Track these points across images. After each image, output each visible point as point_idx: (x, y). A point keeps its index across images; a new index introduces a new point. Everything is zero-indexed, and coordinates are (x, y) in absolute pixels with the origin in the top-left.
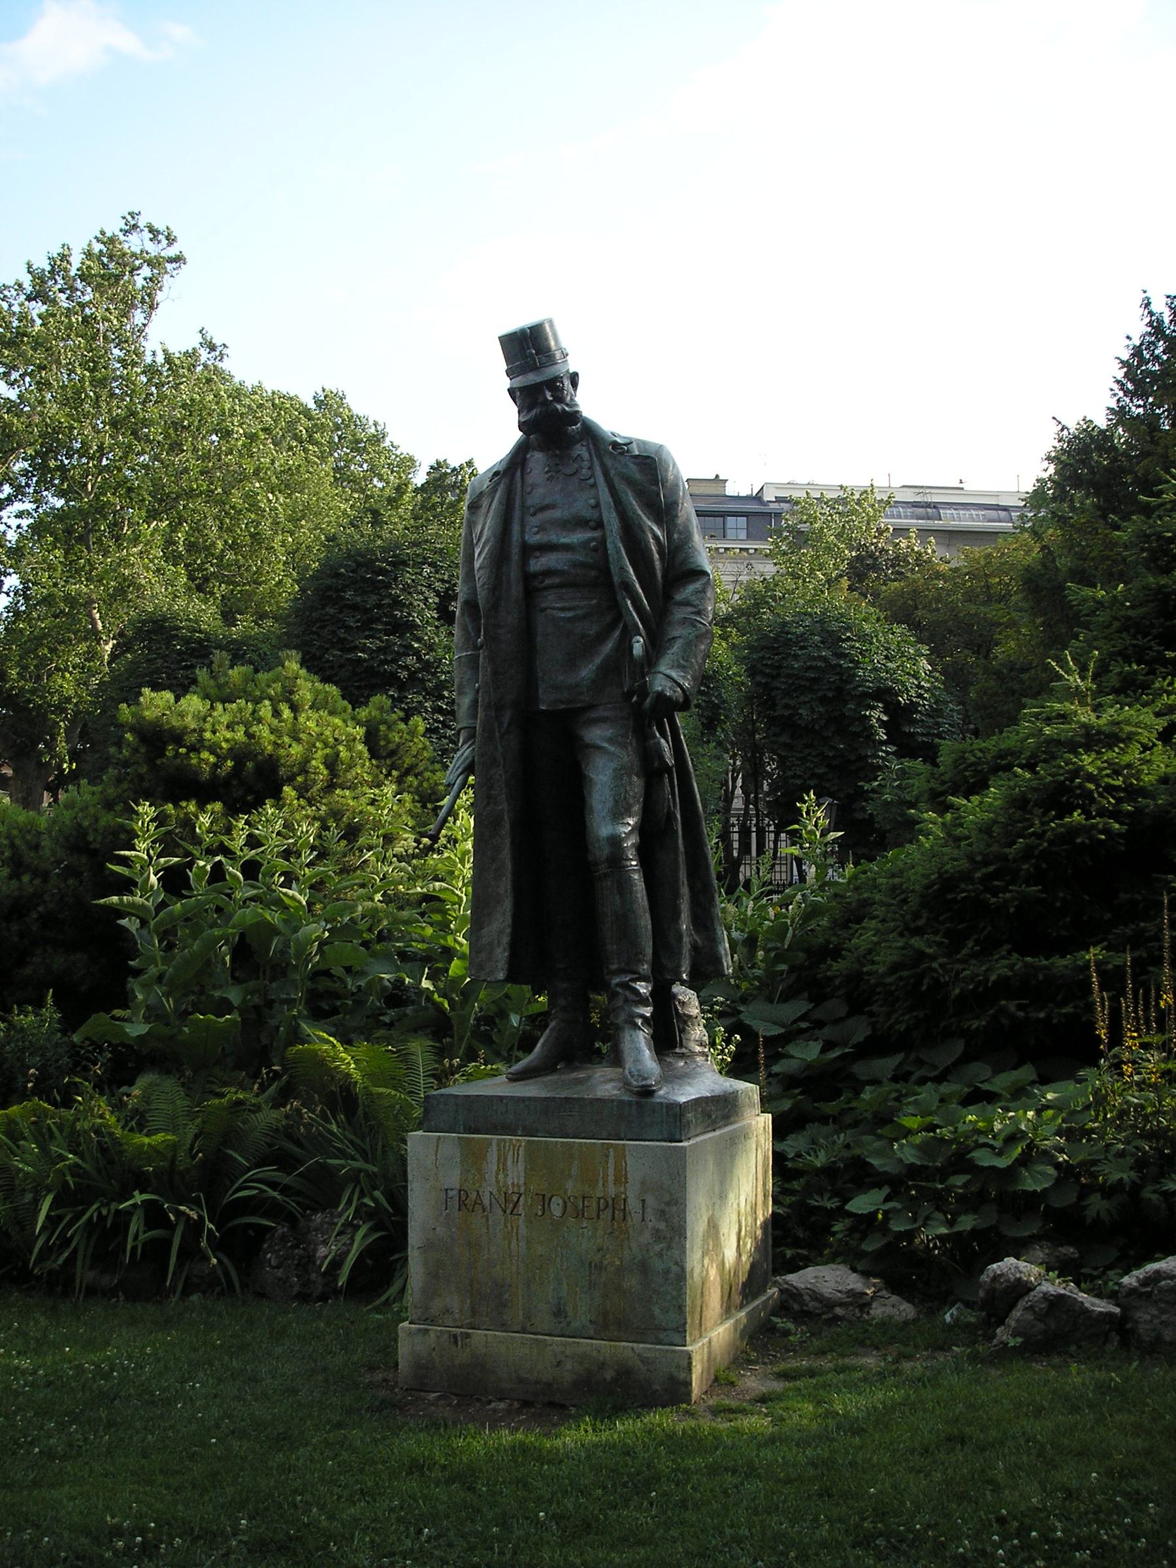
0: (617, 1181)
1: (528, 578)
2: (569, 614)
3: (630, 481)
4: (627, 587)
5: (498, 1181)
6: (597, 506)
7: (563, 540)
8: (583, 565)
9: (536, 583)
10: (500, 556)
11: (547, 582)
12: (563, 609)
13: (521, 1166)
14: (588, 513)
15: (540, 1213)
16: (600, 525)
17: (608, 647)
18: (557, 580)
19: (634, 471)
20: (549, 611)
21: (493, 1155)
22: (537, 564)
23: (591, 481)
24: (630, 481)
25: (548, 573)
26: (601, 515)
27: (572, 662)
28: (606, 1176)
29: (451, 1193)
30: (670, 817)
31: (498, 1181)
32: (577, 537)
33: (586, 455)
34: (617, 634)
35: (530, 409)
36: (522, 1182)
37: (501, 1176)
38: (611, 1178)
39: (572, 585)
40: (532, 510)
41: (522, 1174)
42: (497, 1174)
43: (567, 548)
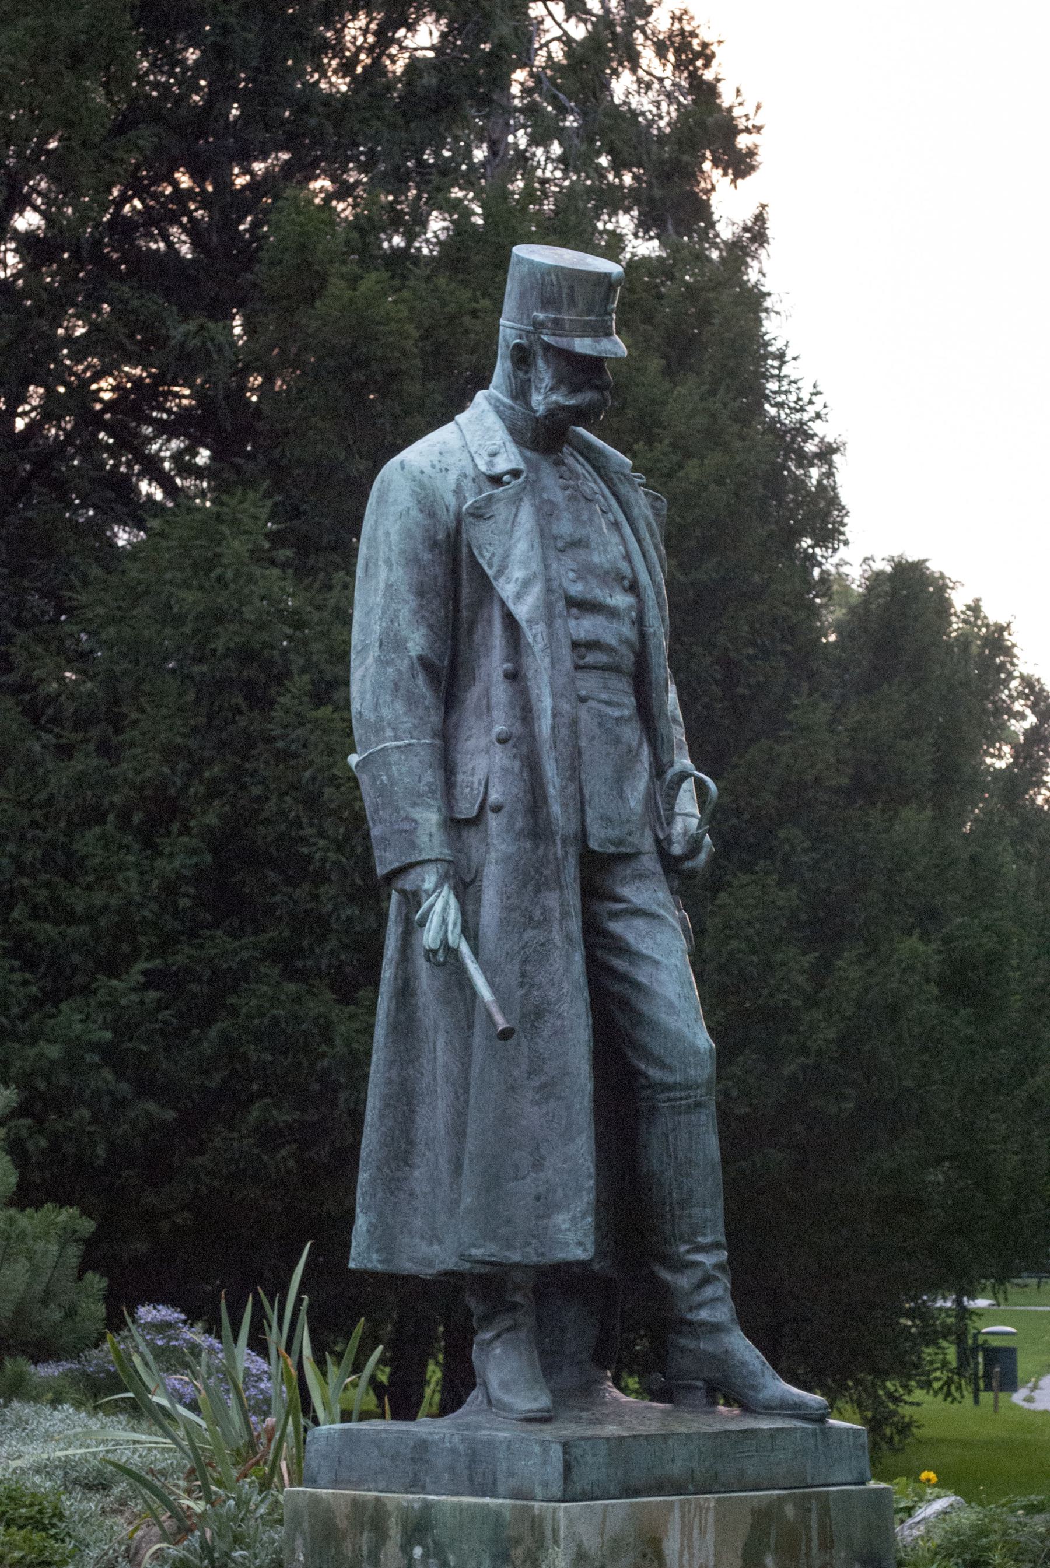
2: (616, 713)
6: (628, 557)
8: (626, 642)
13: (710, 1536)
14: (624, 567)
16: (633, 588)
18: (603, 658)
20: (591, 703)
22: (586, 627)
28: (809, 1540)
37: (686, 1556)
38: (815, 1543)
40: (560, 544)
42: (681, 1555)
43: (613, 613)
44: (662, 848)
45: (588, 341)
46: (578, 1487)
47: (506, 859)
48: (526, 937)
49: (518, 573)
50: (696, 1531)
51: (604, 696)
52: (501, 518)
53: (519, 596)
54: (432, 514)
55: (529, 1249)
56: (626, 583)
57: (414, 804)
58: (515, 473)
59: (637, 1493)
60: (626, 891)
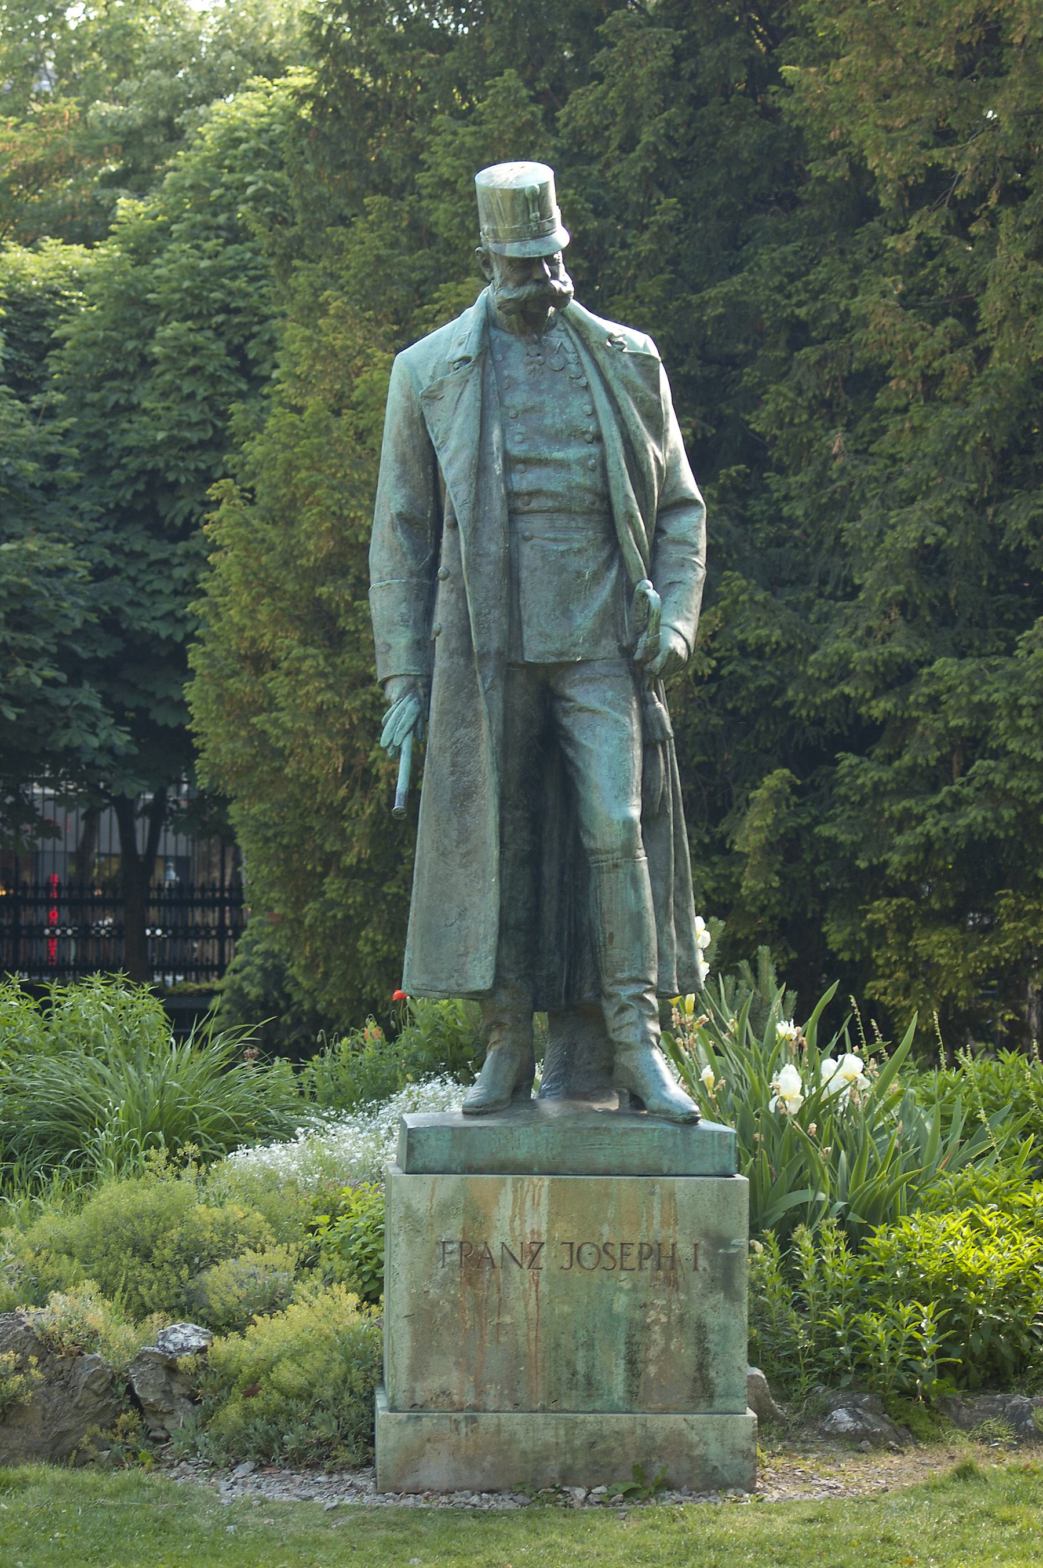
0: (665, 1223)
1: (511, 495)
2: (563, 547)
3: (629, 386)
4: (630, 517)
5: (512, 1230)
6: (594, 413)
7: (558, 455)
8: (579, 486)
9: (519, 504)
10: (480, 468)
11: (534, 505)
12: (555, 540)
13: (544, 1208)
15: (567, 1265)
16: (598, 438)
17: (604, 593)
18: (550, 503)
19: (633, 373)
21: (507, 1198)
22: (524, 481)
23: (583, 382)
24: (629, 386)
25: (532, 494)
26: (598, 426)
27: (564, 605)
28: (650, 1217)
29: (449, 1248)
30: (664, 796)
31: (512, 1230)
32: (573, 453)
33: (568, 345)
34: (613, 573)
35: (520, 284)
36: (544, 1228)
37: (517, 1222)
39: (568, 511)
41: (545, 1219)
42: (512, 1221)
44: (627, 652)
45: (516, 245)
46: (420, 1163)
47: (444, 671)
48: (457, 734)
49: (453, 443)
50: (528, 1204)
51: (551, 536)
52: (447, 399)
53: (450, 463)
54: (409, 398)
55: (452, 981)
56: (588, 437)
57: (389, 632)
58: (465, 360)
59: (480, 1171)
60: (569, 692)
